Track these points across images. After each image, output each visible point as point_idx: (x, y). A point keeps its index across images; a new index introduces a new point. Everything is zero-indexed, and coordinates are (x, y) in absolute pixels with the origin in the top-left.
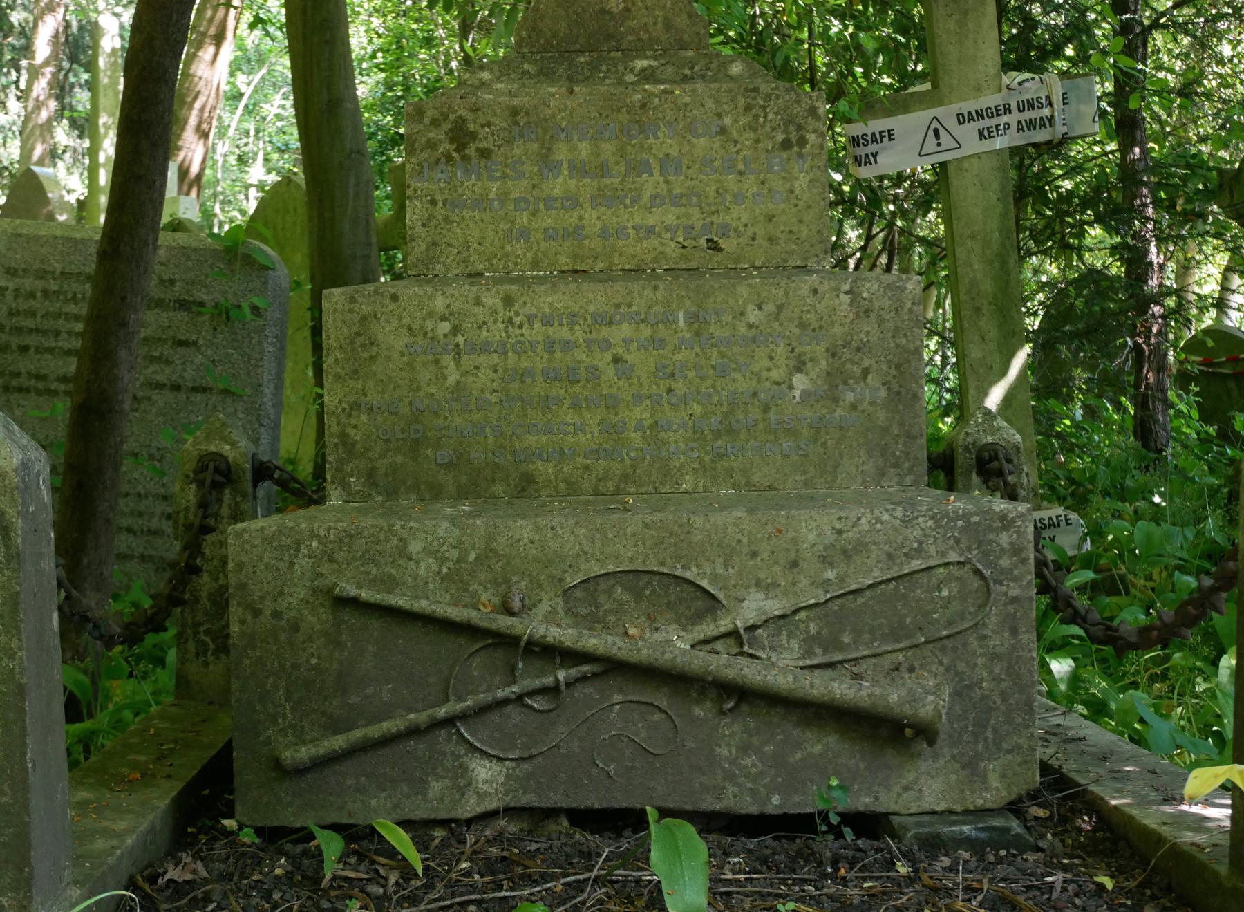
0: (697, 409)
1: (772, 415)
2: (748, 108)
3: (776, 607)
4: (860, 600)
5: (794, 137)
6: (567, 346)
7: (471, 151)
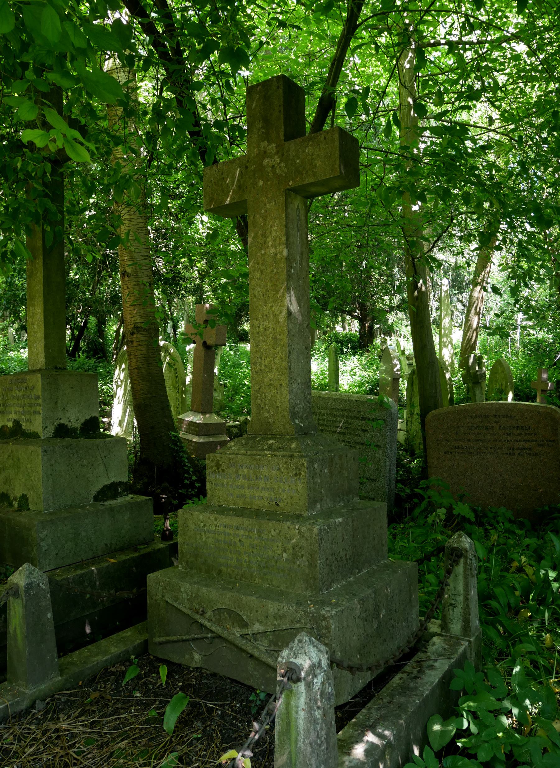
0: (259, 559)
1: (278, 564)
2: (286, 462)
3: (261, 629)
4: (284, 633)
5: (298, 472)
6: (229, 534)
7: (220, 470)
